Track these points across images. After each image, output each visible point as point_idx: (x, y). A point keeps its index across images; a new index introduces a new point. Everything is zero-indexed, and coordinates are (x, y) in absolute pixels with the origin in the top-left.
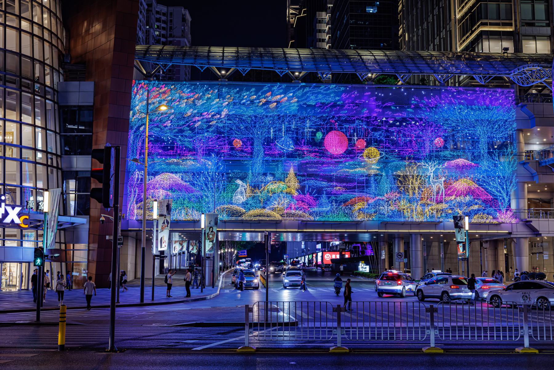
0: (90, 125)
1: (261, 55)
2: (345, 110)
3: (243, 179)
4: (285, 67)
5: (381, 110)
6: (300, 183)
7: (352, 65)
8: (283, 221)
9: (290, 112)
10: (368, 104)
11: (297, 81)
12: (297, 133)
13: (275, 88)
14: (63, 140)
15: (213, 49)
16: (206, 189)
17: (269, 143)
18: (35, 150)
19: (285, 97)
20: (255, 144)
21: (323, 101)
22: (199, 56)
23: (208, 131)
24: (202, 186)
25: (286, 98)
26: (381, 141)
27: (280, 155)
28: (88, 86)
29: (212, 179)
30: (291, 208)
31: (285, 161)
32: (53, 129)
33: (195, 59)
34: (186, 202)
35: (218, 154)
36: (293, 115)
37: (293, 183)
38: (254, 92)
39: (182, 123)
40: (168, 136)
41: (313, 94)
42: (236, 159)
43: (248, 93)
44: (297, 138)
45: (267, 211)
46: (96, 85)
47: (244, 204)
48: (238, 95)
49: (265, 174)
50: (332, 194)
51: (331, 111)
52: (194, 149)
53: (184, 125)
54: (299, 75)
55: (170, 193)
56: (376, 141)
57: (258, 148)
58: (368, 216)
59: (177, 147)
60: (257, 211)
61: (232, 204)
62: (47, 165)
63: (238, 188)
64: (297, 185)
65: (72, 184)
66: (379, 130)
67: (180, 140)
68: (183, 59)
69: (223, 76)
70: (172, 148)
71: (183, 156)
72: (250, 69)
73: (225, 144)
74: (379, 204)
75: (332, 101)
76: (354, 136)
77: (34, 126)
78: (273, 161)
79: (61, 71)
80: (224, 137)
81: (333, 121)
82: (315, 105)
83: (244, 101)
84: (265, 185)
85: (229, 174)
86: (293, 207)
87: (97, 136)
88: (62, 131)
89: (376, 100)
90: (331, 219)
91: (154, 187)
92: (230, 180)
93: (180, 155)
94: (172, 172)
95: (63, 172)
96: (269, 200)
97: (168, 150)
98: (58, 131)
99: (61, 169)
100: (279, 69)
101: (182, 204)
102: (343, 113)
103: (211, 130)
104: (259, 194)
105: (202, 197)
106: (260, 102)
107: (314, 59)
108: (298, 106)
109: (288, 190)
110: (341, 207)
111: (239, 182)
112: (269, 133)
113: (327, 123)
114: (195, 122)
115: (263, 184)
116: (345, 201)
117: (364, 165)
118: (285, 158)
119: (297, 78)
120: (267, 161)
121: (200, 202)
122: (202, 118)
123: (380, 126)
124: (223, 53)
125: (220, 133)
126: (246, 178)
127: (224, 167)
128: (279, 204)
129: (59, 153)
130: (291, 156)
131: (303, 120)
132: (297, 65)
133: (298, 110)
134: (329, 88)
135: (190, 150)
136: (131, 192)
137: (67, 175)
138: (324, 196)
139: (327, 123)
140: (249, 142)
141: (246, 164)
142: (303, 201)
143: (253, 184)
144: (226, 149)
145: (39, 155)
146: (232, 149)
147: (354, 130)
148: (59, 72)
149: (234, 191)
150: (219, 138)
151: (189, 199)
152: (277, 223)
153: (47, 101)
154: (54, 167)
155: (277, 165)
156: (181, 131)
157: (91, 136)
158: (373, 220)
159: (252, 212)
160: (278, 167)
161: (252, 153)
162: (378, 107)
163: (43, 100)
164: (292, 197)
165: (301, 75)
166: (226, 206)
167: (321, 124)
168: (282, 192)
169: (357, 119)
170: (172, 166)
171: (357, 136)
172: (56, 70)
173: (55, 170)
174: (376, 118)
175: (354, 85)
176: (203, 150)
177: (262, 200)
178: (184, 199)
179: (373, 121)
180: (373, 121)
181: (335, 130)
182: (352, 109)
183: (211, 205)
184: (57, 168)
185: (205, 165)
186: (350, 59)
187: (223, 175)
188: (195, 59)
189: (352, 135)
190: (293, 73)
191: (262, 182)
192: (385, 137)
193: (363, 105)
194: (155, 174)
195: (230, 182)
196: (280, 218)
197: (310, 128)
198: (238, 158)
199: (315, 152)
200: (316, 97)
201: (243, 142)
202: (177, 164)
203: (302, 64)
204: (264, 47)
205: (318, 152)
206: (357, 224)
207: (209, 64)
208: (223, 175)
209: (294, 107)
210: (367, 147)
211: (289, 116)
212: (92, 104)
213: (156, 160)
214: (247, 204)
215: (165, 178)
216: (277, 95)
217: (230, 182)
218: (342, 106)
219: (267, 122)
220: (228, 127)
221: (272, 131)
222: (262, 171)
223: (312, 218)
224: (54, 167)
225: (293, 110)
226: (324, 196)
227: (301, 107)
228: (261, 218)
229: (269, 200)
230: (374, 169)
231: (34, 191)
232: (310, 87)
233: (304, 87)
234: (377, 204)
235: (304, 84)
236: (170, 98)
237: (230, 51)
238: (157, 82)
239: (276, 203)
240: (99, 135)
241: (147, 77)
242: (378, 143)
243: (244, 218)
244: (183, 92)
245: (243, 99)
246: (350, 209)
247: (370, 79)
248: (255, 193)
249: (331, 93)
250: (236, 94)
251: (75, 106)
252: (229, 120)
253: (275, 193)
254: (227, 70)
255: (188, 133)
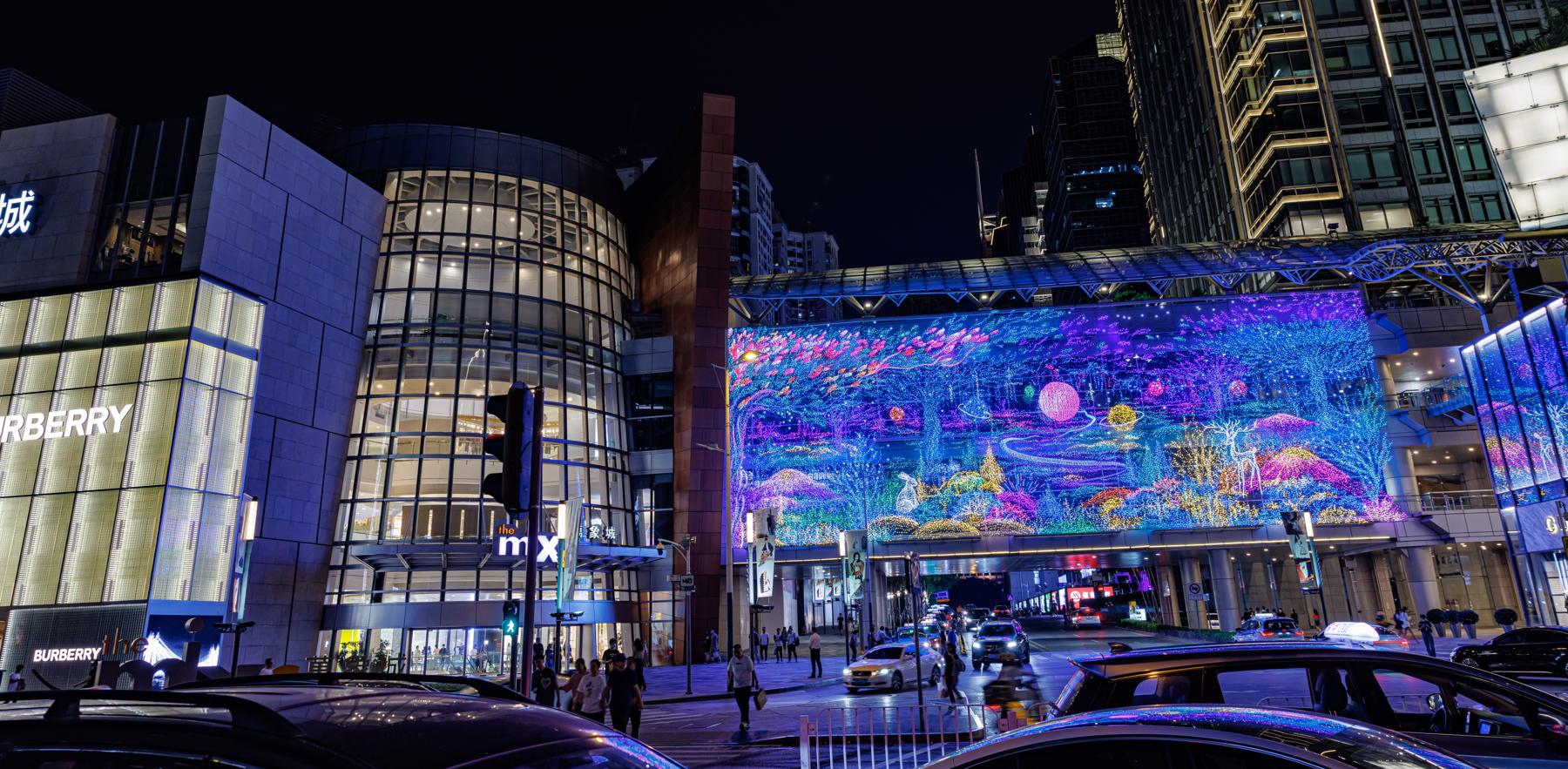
0: (668, 401)
1: (924, 273)
2: (1067, 347)
3: (910, 471)
4: (961, 286)
5: (1129, 343)
6: (1005, 471)
7: (1072, 274)
8: (983, 538)
9: (978, 359)
10: (1106, 334)
11: (985, 308)
12: (992, 390)
13: (950, 322)
14: (631, 429)
15: (849, 272)
16: (851, 491)
17: (948, 409)
18: (588, 445)
19: (967, 334)
20: (926, 412)
21: (1030, 336)
22: (828, 283)
23: (848, 398)
24: (844, 487)
25: (969, 336)
26: (1136, 394)
27: (969, 428)
28: (665, 343)
29: (861, 476)
30: (994, 515)
31: (977, 437)
32: (615, 412)
33: (821, 288)
34: (821, 514)
35: (867, 433)
36: (984, 363)
37: (994, 473)
38: (918, 330)
39: (807, 388)
40: (787, 411)
41: (1012, 325)
42: (896, 439)
43: (907, 333)
44: (993, 399)
45: (954, 522)
46: (676, 341)
47: (916, 513)
48: (892, 338)
49: (946, 461)
50: (1061, 488)
51: (1045, 351)
52: (829, 428)
53: (811, 391)
54: (988, 300)
55: (794, 501)
56: (1127, 394)
57: (932, 419)
58: (1129, 522)
59: (802, 427)
60: (939, 523)
61: (895, 513)
62: (607, 469)
63: (903, 487)
64: (1000, 476)
65: (646, 497)
66: (1131, 375)
67: (805, 415)
68: (804, 289)
69: (868, 312)
70: (795, 429)
71: (813, 440)
72: (906, 295)
73: (877, 417)
74: (1145, 500)
75: (1044, 336)
76: (1088, 388)
77: (586, 409)
78: (957, 439)
79: (626, 324)
80: (873, 405)
81: (1051, 367)
82: (1018, 344)
83: (903, 346)
84: (947, 480)
85: (886, 464)
86: (997, 514)
87: (679, 419)
88: (630, 414)
89: (1119, 327)
90: (1064, 531)
91: (769, 494)
92: (889, 474)
93: (808, 439)
94: (796, 468)
95: (632, 478)
96: (956, 504)
97: (789, 432)
98: (622, 414)
99: (629, 473)
100: (952, 290)
101: (815, 518)
102: (1066, 353)
103: (853, 395)
104: (939, 494)
105: (846, 504)
106: (928, 345)
107: (1009, 271)
108: (990, 347)
109: (986, 485)
110: (1079, 508)
111: (904, 476)
112: (947, 393)
113: (1040, 371)
114: (828, 385)
115: (944, 478)
116: (1085, 498)
117: (1111, 435)
118: (977, 432)
119: (985, 304)
120: (947, 440)
121: (843, 513)
122: (837, 377)
123: (1131, 369)
124: (865, 275)
125: (868, 399)
126: (915, 469)
127: (878, 454)
128: (972, 509)
129: (625, 449)
130: (984, 428)
131: (1001, 368)
132: (983, 282)
133: (991, 354)
134: (1038, 314)
135: (822, 431)
136: (734, 503)
137: (638, 482)
138: (1048, 491)
139: (1040, 371)
140: (915, 410)
141: (914, 447)
142: (1013, 503)
143: (927, 479)
144: (879, 425)
145: (597, 453)
146: (889, 423)
147: (1088, 381)
148: (624, 327)
149: (897, 491)
150: (867, 407)
151: (826, 508)
152: (972, 542)
153: (605, 370)
154: (618, 471)
155: (964, 445)
156: (806, 401)
157: (672, 418)
158: (1138, 529)
159: (928, 526)
160: (966, 448)
161: (921, 428)
162: (1123, 337)
163: (599, 369)
164: (994, 496)
165: (991, 299)
166: (886, 518)
167: (1030, 374)
168: (976, 489)
169: (1091, 360)
170: (796, 458)
171: (1094, 388)
172: (617, 323)
173: (619, 475)
174: (1122, 355)
175: (1079, 307)
176: (843, 429)
177: (945, 505)
178: (818, 510)
179: (1118, 362)
180: (1118, 362)
181: (1055, 380)
182: (1080, 346)
183: (861, 518)
184: (623, 472)
185: (848, 451)
186: (1067, 265)
187: (877, 467)
188: (821, 288)
189: (1084, 388)
190: (978, 295)
191: (942, 474)
192: (1143, 387)
193: (1099, 337)
194: (770, 473)
195: (890, 477)
196: (978, 533)
197: (1013, 381)
198: (900, 438)
199: (1026, 419)
200: (1019, 330)
201: (906, 411)
202: (804, 454)
203: (989, 280)
204: (929, 262)
205: (1030, 419)
206: (1111, 537)
207: (843, 293)
208: (877, 467)
209: (985, 349)
210: (1112, 404)
211: (977, 364)
212: (671, 370)
213: (771, 450)
214: (921, 512)
215: (786, 479)
216: (954, 332)
217: (890, 477)
218: (1062, 342)
219: (942, 377)
220: (880, 388)
221: (951, 390)
222: (940, 458)
223: (1032, 531)
224: (618, 471)
225: (984, 354)
226: (1048, 491)
227: (995, 350)
228: (945, 535)
229: (956, 504)
230: (1130, 441)
231: (587, 509)
232: (1006, 315)
233: (996, 316)
234: (1141, 500)
235: (996, 312)
236: (787, 351)
237: (876, 272)
238: (766, 329)
239: (969, 508)
240: (682, 416)
241: (753, 323)
242: (1132, 397)
243: (916, 535)
244: (807, 340)
245: (901, 344)
246: (1096, 511)
247: (1105, 295)
248: (933, 493)
249: (1042, 322)
250: (889, 335)
251: (646, 375)
252: (882, 377)
253: (965, 492)
254: (874, 300)
255: (818, 403)
